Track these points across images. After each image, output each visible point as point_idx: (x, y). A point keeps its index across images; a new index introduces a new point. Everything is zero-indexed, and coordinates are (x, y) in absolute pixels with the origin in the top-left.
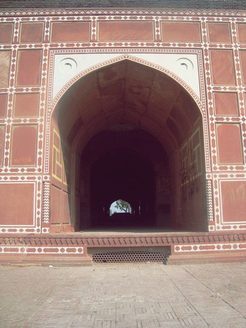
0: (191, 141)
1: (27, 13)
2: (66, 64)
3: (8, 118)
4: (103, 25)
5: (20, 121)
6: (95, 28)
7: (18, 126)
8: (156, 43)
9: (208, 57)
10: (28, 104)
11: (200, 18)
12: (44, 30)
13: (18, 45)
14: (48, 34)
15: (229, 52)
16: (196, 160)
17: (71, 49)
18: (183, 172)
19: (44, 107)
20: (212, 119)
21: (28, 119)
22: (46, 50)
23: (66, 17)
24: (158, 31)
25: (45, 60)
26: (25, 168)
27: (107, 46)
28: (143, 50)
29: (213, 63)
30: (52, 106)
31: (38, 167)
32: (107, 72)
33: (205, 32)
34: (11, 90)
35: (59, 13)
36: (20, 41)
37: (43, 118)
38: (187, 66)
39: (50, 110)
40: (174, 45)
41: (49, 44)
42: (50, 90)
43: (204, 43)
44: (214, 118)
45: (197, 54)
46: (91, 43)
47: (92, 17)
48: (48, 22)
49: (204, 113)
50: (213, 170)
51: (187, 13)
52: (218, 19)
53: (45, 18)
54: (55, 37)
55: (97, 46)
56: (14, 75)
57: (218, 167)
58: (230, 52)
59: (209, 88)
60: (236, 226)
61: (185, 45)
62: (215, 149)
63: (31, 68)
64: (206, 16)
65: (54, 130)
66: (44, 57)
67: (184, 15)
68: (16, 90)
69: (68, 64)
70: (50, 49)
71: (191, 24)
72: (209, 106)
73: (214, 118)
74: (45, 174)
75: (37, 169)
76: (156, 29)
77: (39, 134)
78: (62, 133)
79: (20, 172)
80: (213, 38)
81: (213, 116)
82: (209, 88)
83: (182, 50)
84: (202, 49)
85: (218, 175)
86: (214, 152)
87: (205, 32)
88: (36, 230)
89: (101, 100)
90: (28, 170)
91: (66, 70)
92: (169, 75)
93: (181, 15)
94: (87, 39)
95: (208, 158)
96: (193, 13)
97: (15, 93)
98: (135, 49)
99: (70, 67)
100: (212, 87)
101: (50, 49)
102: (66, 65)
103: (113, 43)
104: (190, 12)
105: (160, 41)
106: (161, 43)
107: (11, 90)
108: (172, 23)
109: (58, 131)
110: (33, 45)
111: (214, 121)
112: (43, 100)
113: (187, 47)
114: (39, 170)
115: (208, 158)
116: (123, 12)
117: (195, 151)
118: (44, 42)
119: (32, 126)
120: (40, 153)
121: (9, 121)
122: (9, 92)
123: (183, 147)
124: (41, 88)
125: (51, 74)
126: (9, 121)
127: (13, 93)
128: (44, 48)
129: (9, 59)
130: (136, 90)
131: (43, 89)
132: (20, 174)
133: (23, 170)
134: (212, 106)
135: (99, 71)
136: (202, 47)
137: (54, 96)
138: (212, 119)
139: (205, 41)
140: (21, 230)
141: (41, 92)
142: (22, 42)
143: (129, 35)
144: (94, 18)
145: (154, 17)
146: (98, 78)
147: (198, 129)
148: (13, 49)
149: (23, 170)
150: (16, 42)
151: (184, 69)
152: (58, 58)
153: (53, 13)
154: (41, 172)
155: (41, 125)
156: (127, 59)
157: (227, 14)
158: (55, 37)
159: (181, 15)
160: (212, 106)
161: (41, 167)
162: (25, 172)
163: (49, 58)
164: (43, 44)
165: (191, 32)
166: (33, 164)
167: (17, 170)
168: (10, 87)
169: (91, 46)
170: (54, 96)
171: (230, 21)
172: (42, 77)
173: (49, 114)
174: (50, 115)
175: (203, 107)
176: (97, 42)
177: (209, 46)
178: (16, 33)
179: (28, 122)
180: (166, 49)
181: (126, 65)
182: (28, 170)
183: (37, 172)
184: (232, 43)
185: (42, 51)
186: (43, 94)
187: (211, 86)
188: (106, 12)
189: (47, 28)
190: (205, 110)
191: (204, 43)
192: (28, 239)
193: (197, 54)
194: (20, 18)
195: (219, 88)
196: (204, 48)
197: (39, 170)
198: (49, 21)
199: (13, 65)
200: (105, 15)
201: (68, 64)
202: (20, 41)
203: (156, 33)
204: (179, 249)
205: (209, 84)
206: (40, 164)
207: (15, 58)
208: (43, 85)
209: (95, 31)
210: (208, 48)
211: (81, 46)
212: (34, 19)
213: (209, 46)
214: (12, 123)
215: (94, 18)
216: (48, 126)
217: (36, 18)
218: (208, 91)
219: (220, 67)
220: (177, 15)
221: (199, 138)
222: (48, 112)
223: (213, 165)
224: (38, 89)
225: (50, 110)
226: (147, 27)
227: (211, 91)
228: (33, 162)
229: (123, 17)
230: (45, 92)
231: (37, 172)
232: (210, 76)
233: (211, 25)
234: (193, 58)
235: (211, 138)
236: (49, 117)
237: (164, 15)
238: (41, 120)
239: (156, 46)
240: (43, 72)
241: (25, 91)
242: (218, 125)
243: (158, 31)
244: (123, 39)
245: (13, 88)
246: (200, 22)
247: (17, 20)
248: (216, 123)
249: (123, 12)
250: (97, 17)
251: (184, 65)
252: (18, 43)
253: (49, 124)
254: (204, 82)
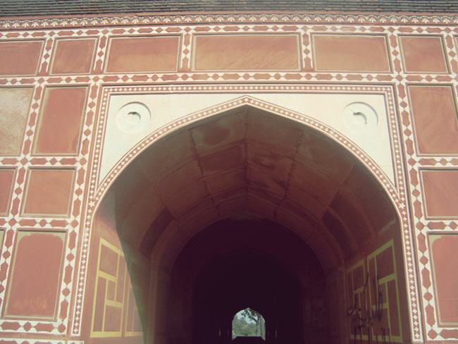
0: (372, 262)
1: (69, 22)
2: (130, 113)
3: (11, 216)
4: (204, 42)
5: (34, 223)
6: (189, 48)
7: (29, 234)
8: (303, 74)
9: (406, 100)
10: (51, 190)
11: (386, 27)
12: (96, 52)
13: (46, 78)
14: (102, 58)
16: (386, 306)
17: (141, 87)
18: (355, 313)
19: (81, 197)
20: (421, 226)
21: (49, 220)
22: (95, 88)
23: (137, 29)
24: (307, 52)
25: (92, 105)
26: (34, 323)
27: (211, 80)
29: (415, 112)
30: (97, 196)
31: (59, 321)
32: (210, 128)
33: (397, 53)
34: (24, 162)
35: (125, 22)
36: (51, 71)
37: (78, 219)
38: (366, 119)
39: (92, 204)
40: (339, 77)
41: (101, 76)
42: (95, 163)
43: (396, 74)
44: (425, 223)
45: (384, 94)
46: (180, 75)
47: (183, 27)
48: (104, 39)
49: (404, 213)
50: (429, 339)
51: (362, 20)
52: (420, 30)
53: (101, 30)
54: (113, 64)
55: (190, 80)
56: (31, 134)
57: (438, 330)
58: (447, 90)
59: (412, 162)
61: (361, 78)
62: (431, 290)
63: (64, 119)
64: (397, 24)
65: (103, 242)
66: (90, 100)
67: (356, 23)
68: (32, 162)
69: (134, 113)
70: (104, 85)
71: (368, 38)
72: (413, 199)
73: (425, 223)
74: (73, 338)
75: (56, 325)
76: (304, 47)
77: (68, 251)
78: (126, 241)
79: (21, 330)
80: (412, 64)
81: (423, 220)
82: (412, 162)
83: (354, 86)
84: (393, 85)
86: (428, 297)
89: (203, 177)
90: (39, 327)
91: (131, 123)
92: (331, 135)
93: (349, 23)
94: (172, 67)
95: (415, 311)
96: (372, 20)
97: (31, 168)
99: (138, 117)
100: (417, 159)
101: (104, 85)
102: (131, 115)
103: (221, 74)
104: (367, 18)
105: (312, 71)
106: (313, 74)
107: (24, 162)
108: (333, 38)
109: (117, 239)
110: (73, 77)
111: (425, 230)
112: (80, 183)
113: (365, 80)
114: (61, 328)
115: (415, 311)
116: (242, 19)
117: (384, 284)
118: (93, 73)
119: (55, 234)
120: (66, 292)
121: (13, 222)
122: (19, 166)
123: (355, 267)
124: (78, 159)
126: (13, 222)
127: (26, 167)
128: (92, 83)
129: (28, 103)
130: (266, 161)
131: (83, 161)
132: (21, 336)
133: (28, 327)
134: (420, 198)
135: (193, 128)
136: (393, 81)
137: (104, 173)
138: (421, 226)
139: (399, 71)
141: (78, 166)
142: (55, 72)
143: (252, 59)
144: (187, 30)
145: (300, 26)
146: (193, 141)
147: (390, 243)
148: (37, 84)
149: (28, 327)
150: (44, 73)
151: (360, 122)
153: (115, 22)
154: (65, 333)
155: (73, 234)
156: (246, 105)
157: (436, 21)
159: (349, 23)
160: (420, 198)
161: (66, 323)
162: (33, 330)
163: (99, 101)
164: (92, 77)
165: (373, 52)
166: (51, 314)
167: (16, 326)
168: (22, 156)
169: (180, 80)
170: (104, 173)
171: (442, 33)
172: (84, 137)
173: (90, 211)
174: (91, 214)
175: (401, 202)
176: (190, 72)
177: (407, 78)
178: (46, 57)
179: (48, 226)
180: (323, 85)
181: (247, 117)
182: (39, 327)
183: (55, 332)
184: (450, 73)
185: (89, 89)
186: (82, 171)
187: (414, 156)
188: (209, 20)
189: (102, 47)
190: (405, 208)
191: (396, 74)
193: (384, 94)
194: (57, 31)
195: (434, 162)
196: (397, 83)
197: (61, 328)
198: (107, 35)
199: (34, 114)
200: (208, 23)
201: (134, 113)
202: (51, 71)
203: (304, 56)
205: (411, 153)
206: (63, 316)
207: (39, 102)
208: (84, 153)
210: (404, 82)
211: (160, 81)
212: (80, 33)
213: (407, 78)
214: (17, 226)
215: (187, 30)
216: (86, 236)
217: (84, 30)
218: (409, 167)
220: (342, 23)
221: (393, 262)
222: (89, 206)
223: (428, 328)
224: (74, 161)
225: (92, 204)
226: (287, 45)
227: (416, 167)
228: (49, 311)
229: (241, 26)
230: (85, 167)
231: (55, 332)
232: (411, 137)
233: (407, 40)
234: (377, 101)
235: (421, 267)
236: (91, 218)
237: (319, 23)
238: (74, 224)
239: (303, 79)
240: (85, 128)
241: (48, 165)
242: (433, 238)
243: (307, 52)
244: (240, 68)
245: (29, 157)
246: (385, 35)
247: (51, 34)
248: (430, 234)
249: (242, 19)
250: (193, 27)
251: (360, 117)
252: (47, 75)
253: (89, 232)
254: (401, 150)
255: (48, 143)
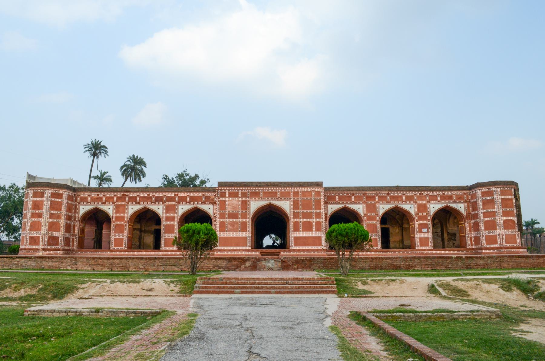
10: (244, 216)
15: (298, 200)
17: (255, 200)
28: (275, 200)
33: (292, 194)
60: (297, 248)
63: (245, 205)
83: (285, 200)
85: (292, 235)
87: (292, 194)
88: (248, 248)
91: (255, 205)
98: (272, 200)
107: (240, 212)
125: (250, 207)
140: (244, 248)
151: (285, 205)
152: (252, 202)
158: (251, 196)
180: (281, 200)
192: (246, 250)
204: (282, 253)
209: (261, 195)
219: (295, 205)
233: (294, 193)
254: (291, 209)
255: (242, 209)
